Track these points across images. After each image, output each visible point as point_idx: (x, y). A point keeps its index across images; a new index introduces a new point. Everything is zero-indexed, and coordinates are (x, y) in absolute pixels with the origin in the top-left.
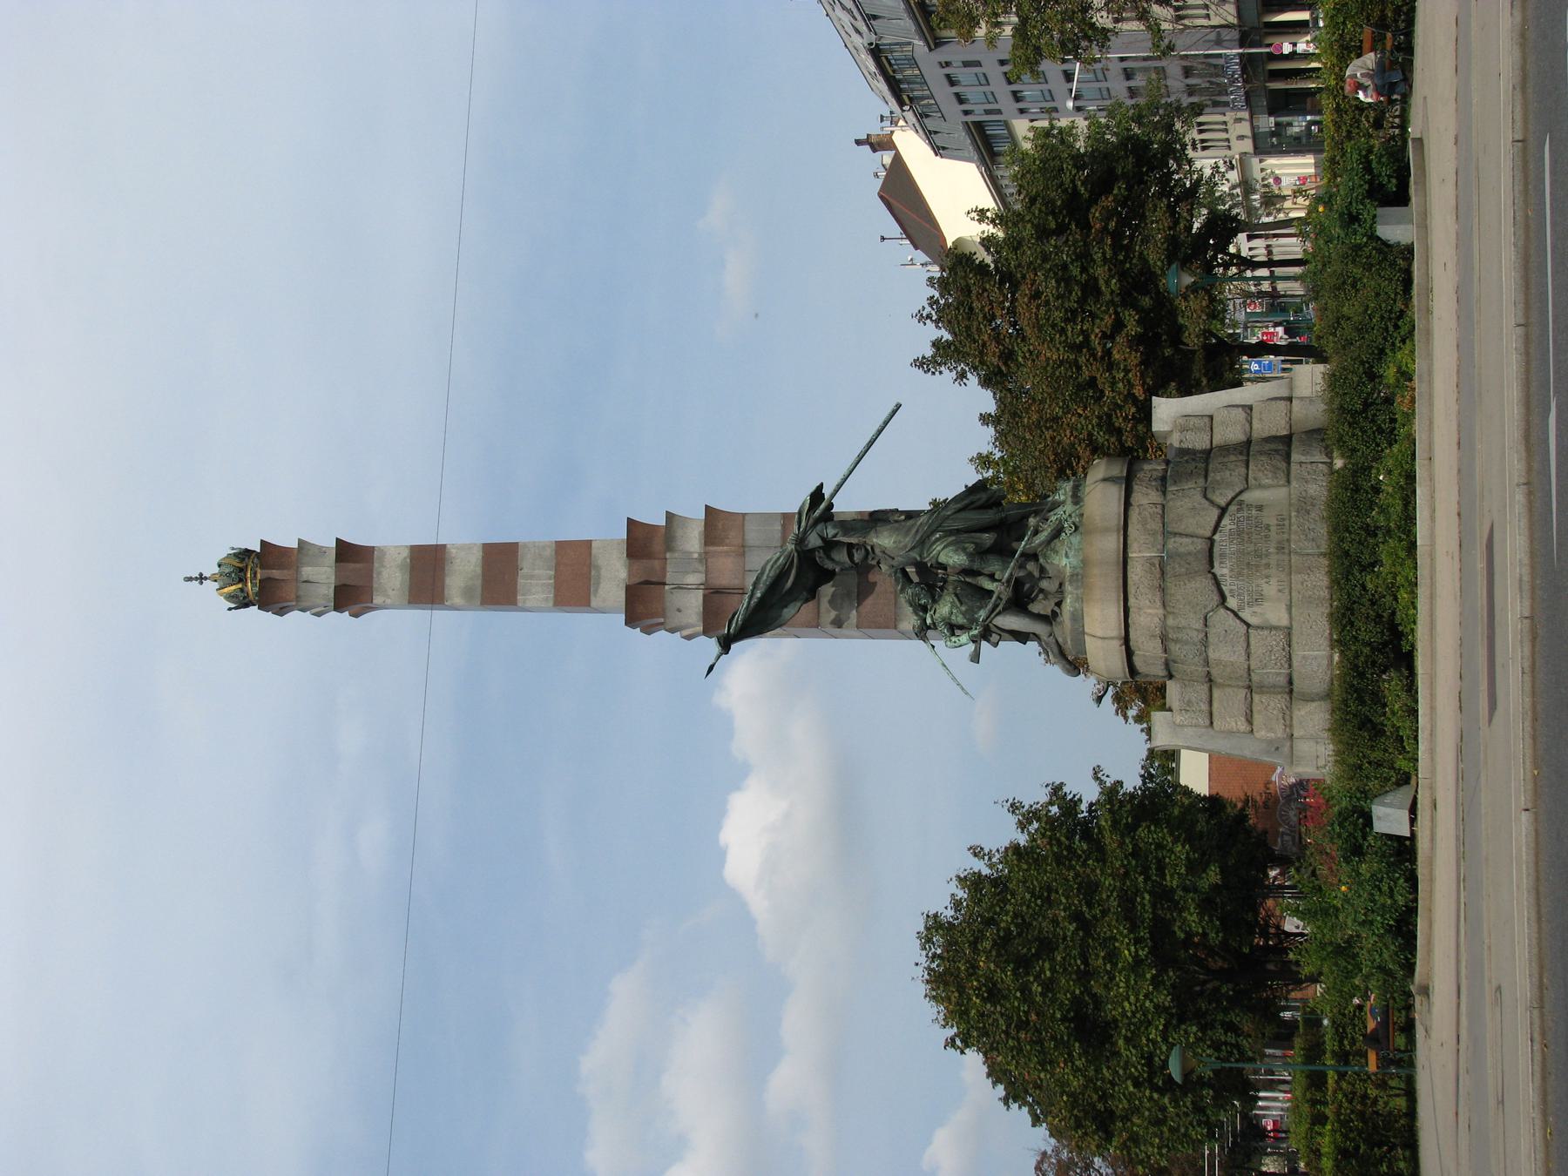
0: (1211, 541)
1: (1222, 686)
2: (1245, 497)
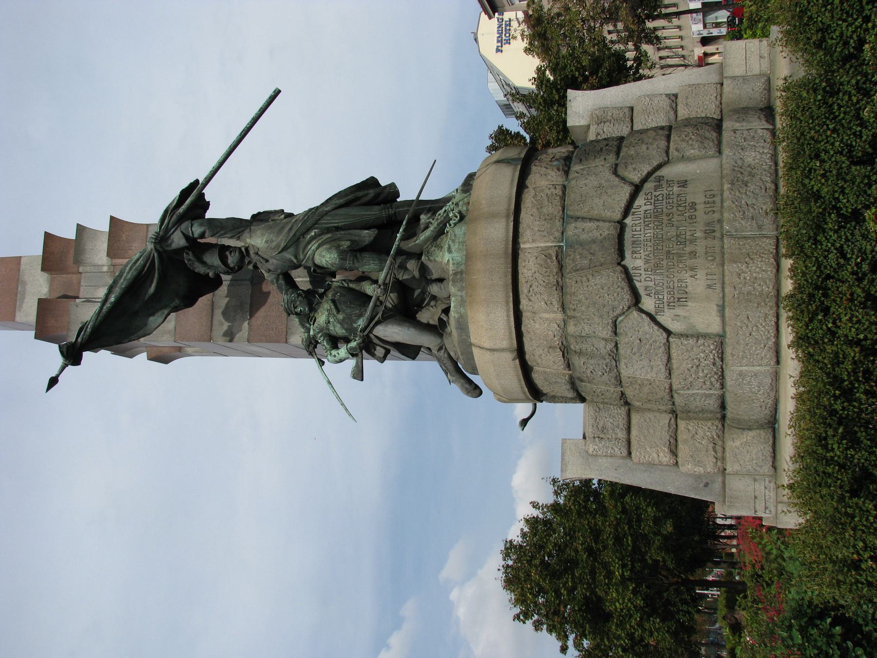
0: (622, 227)
1: (639, 410)
2: (664, 172)
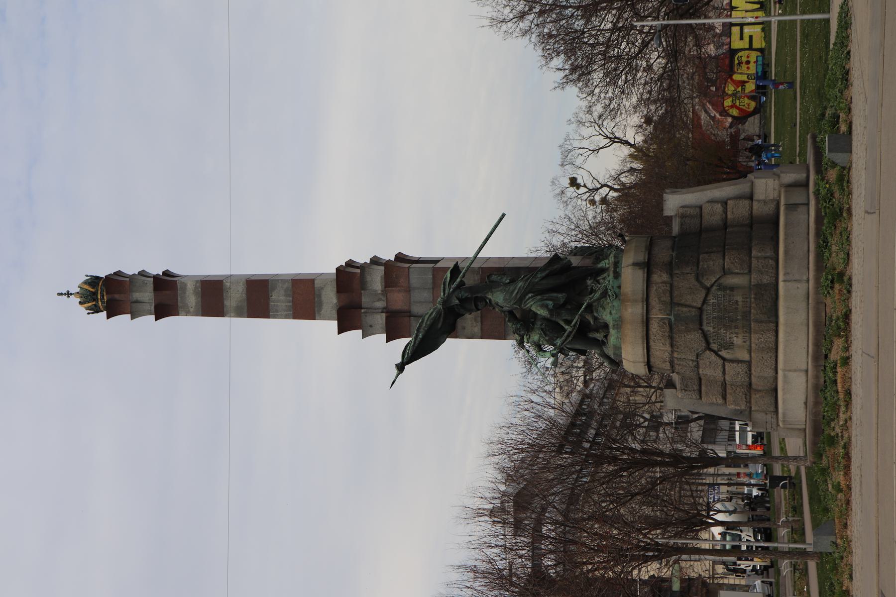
0: (701, 310)
2: (722, 281)
